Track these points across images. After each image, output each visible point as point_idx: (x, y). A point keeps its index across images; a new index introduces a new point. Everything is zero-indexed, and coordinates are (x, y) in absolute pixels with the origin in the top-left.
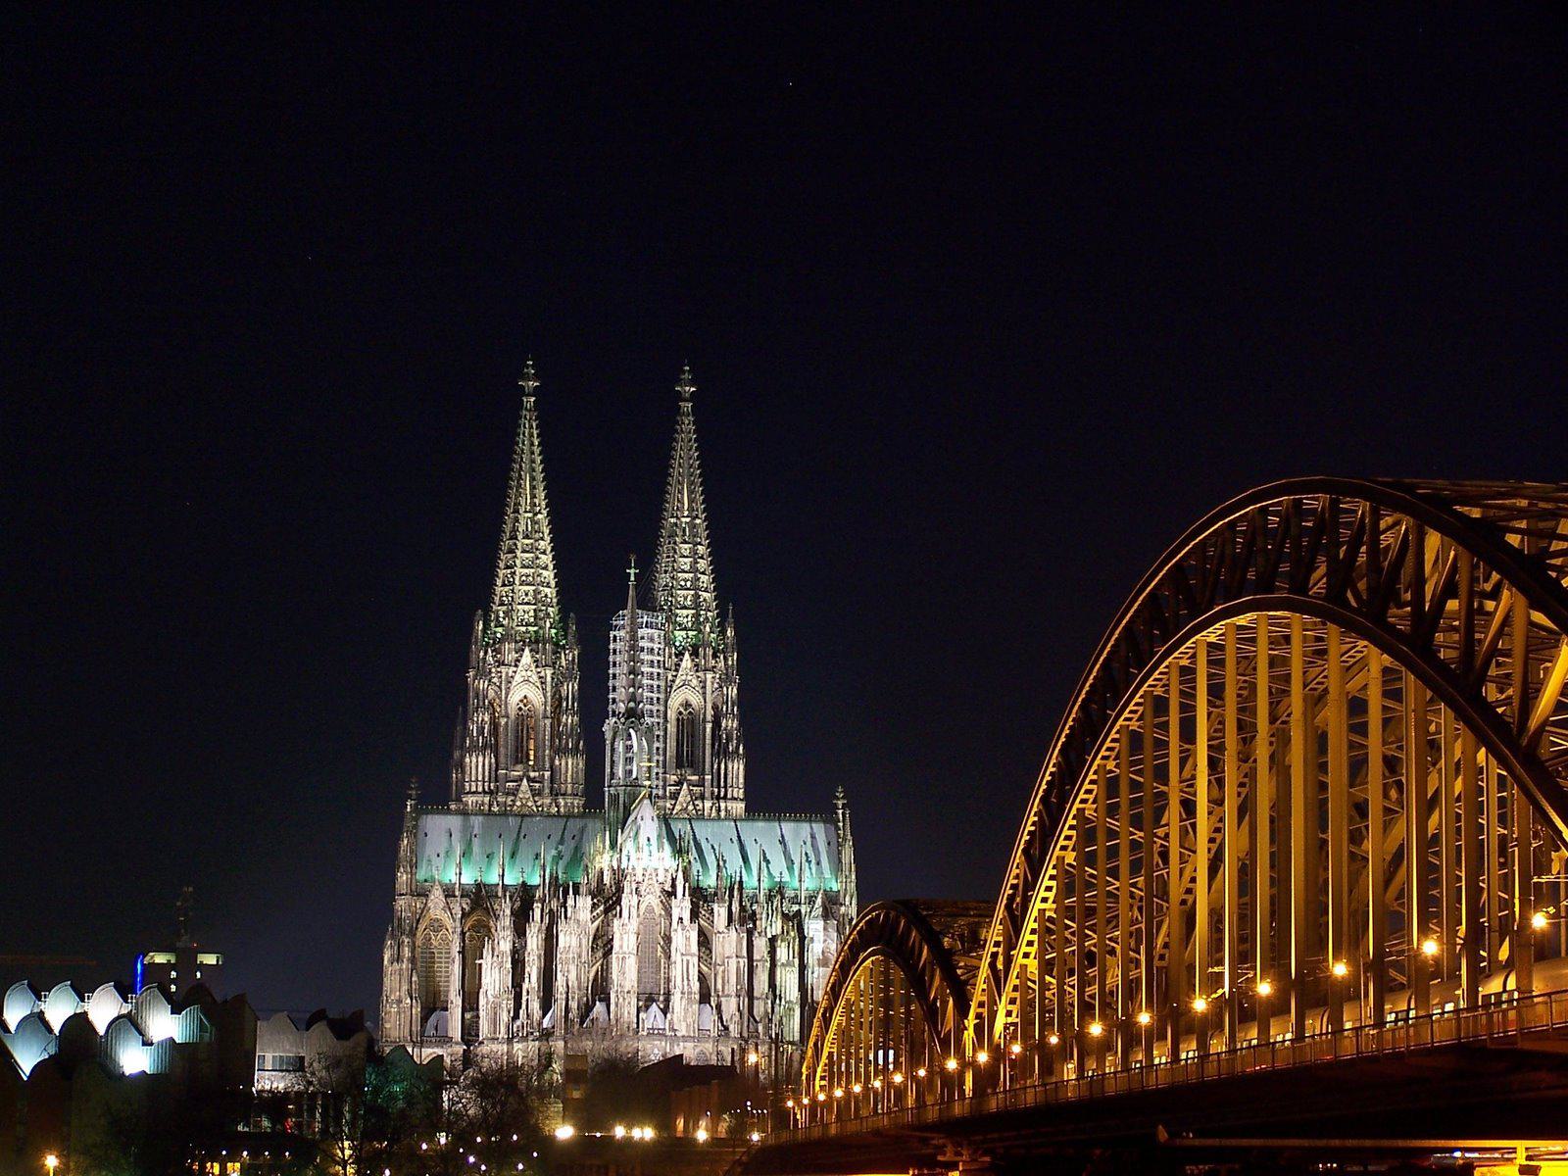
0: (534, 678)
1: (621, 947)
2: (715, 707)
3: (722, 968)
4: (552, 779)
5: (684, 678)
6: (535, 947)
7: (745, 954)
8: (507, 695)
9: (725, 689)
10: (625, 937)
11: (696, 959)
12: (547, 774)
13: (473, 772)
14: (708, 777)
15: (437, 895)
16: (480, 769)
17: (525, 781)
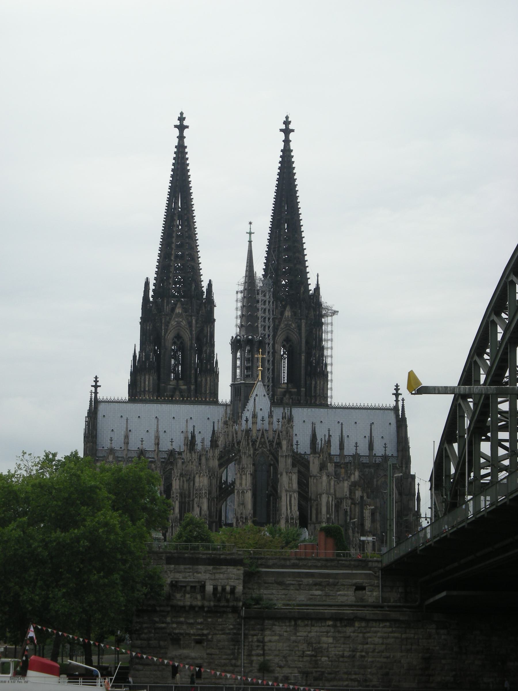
0: (184, 323)
1: (241, 484)
2: (307, 343)
3: (315, 503)
4: (196, 390)
5: (286, 323)
6: (178, 487)
7: (332, 491)
8: (165, 334)
9: (314, 330)
10: (244, 477)
11: (296, 495)
12: (193, 387)
13: (142, 385)
14: (303, 389)
15: (111, 458)
16: (147, 383)
17: (177, 393)
